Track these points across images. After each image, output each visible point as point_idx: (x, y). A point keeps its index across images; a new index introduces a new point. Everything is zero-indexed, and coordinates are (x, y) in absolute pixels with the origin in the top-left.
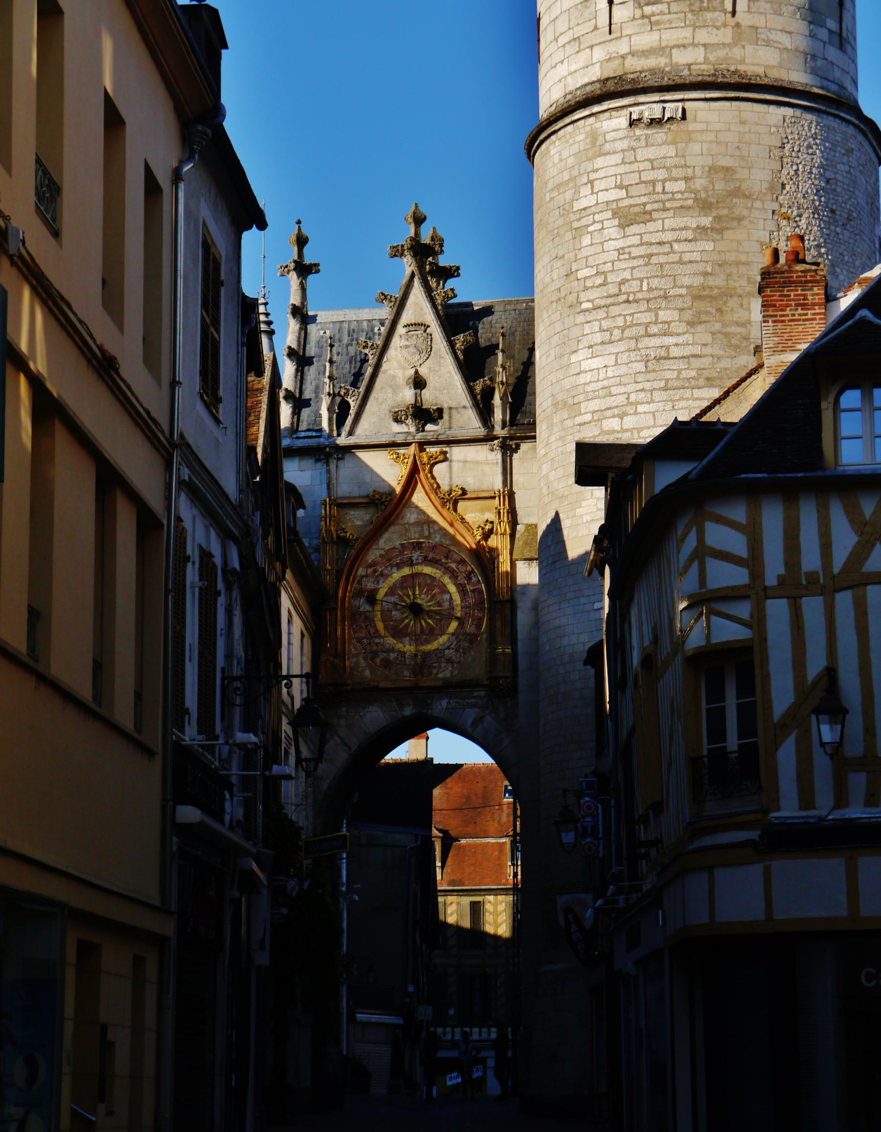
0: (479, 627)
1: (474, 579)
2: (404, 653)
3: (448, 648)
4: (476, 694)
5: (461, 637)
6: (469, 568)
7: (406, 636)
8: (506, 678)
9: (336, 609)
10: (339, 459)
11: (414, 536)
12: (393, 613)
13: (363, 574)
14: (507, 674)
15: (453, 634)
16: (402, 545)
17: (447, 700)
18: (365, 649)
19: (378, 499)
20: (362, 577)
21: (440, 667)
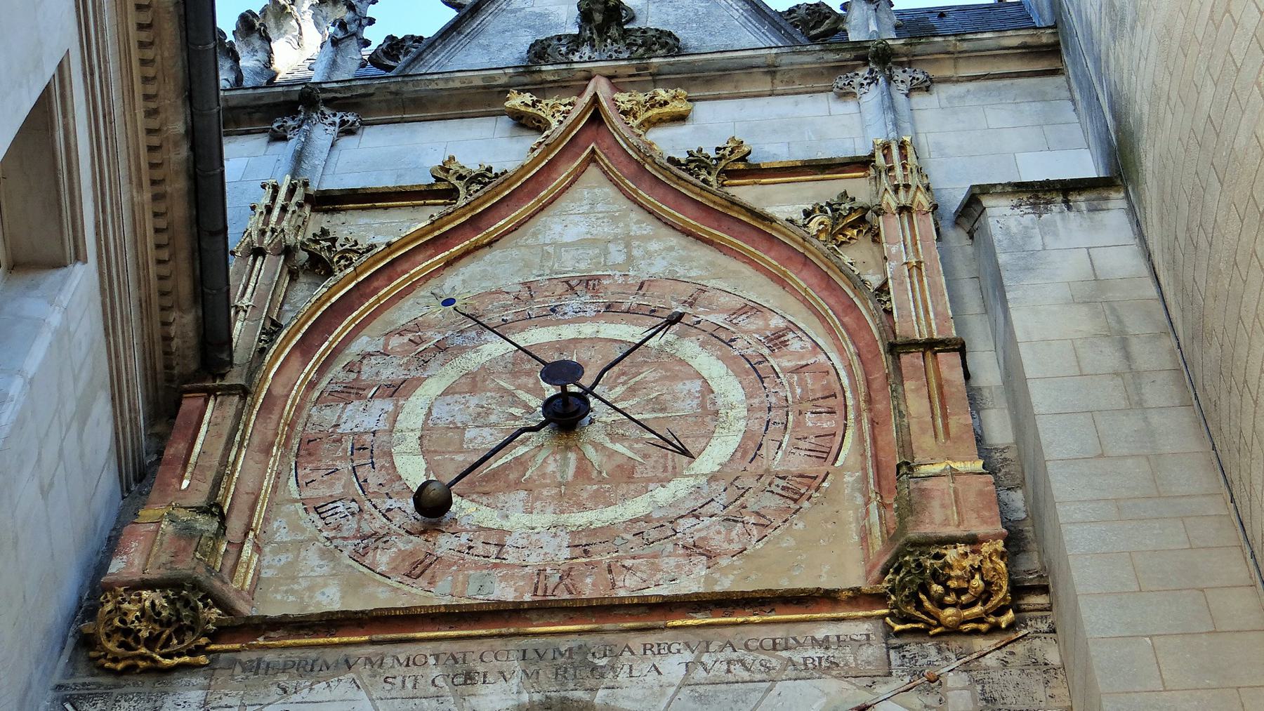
0: (825, 453)
1: (795, 345)
2: (503, 532)
3: (694, 514)
4: (821, 632)
5: (748, 481)
6: (776, 322)
7: (517, 485)
8: (973, 541)
9: (244, 392)
10: (347, 130)
11: (574, 264)
12: (470, 434)
13: (371, 349)
14: (980, 530)
15: (713, 478)
16: (527, 285)
17: (688, 656)
18: (338, 528)
19: (460, 178)
20: (366, 356)
21: (656, 569)
